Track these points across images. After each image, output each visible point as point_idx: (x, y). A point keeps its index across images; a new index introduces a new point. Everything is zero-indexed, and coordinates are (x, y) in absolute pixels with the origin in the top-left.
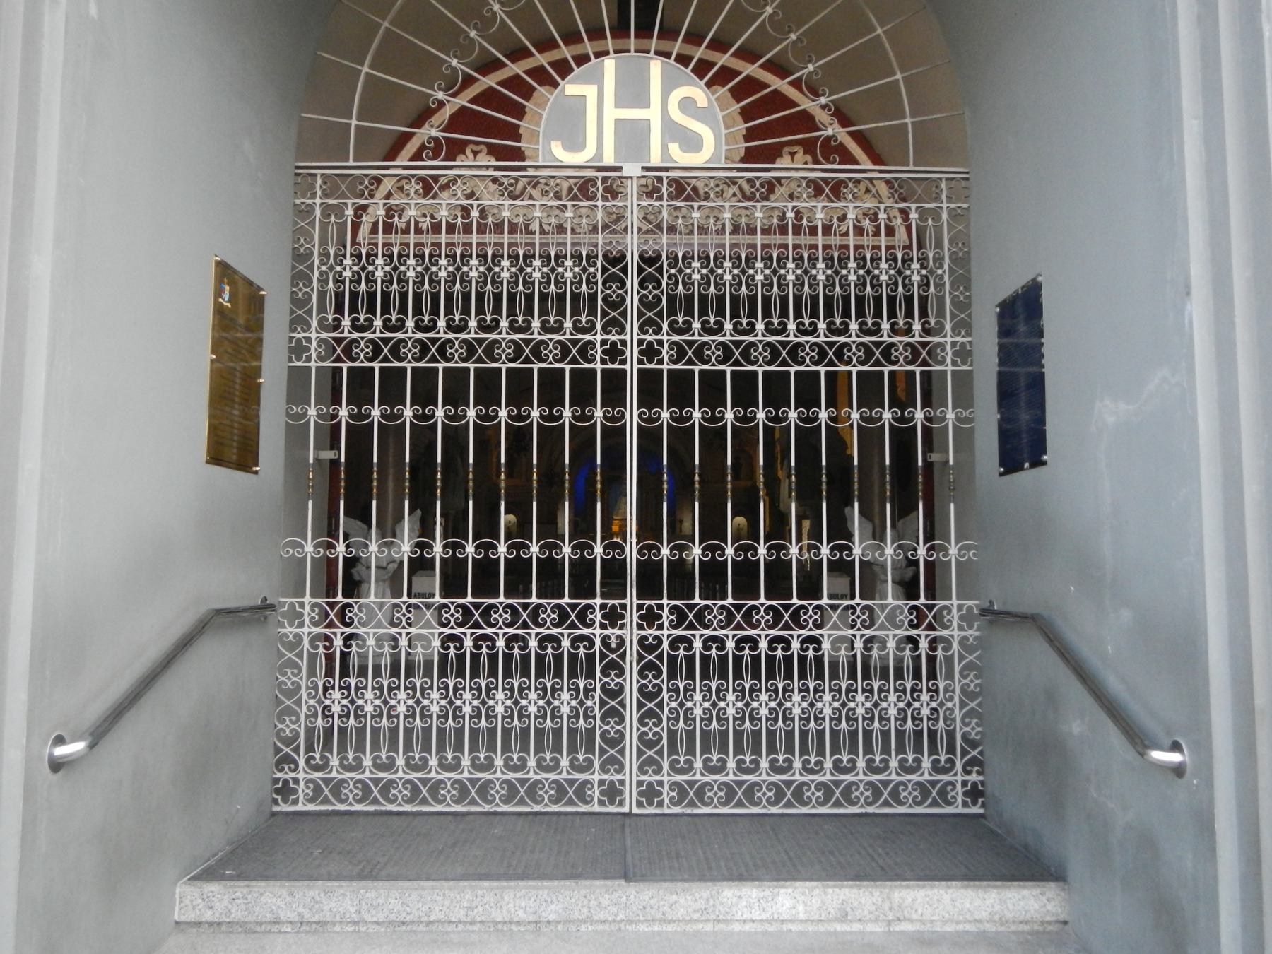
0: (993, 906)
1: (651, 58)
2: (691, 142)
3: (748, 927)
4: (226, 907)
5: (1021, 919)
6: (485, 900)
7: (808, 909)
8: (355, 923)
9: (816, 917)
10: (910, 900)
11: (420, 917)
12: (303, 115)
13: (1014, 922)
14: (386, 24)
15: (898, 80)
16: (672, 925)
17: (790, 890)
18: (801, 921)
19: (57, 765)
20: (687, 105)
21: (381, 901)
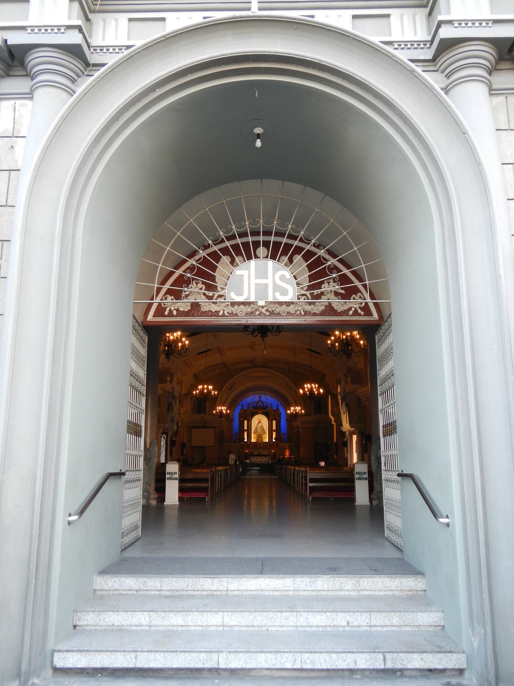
0: (398, 585)
1: (269, 260)
2: (284, 292)
3: (306, 593)
4: (113, 584)
5: (408, 589)
6: (208, 582)
7: (328, 586)
8: (160, 590)
9: (331, 589)
10: (366, 582)
11: (184, 588)
12: (137, 283)
13: (406, 591)
14: (168, 248)
15: (363, 267)
16: (277, 592)
17: (321, 579)
18: (326, 590)
19: (69, 523)
20: (282, 278)
21: (169, 582)
